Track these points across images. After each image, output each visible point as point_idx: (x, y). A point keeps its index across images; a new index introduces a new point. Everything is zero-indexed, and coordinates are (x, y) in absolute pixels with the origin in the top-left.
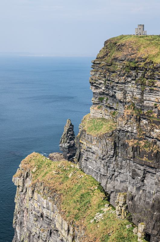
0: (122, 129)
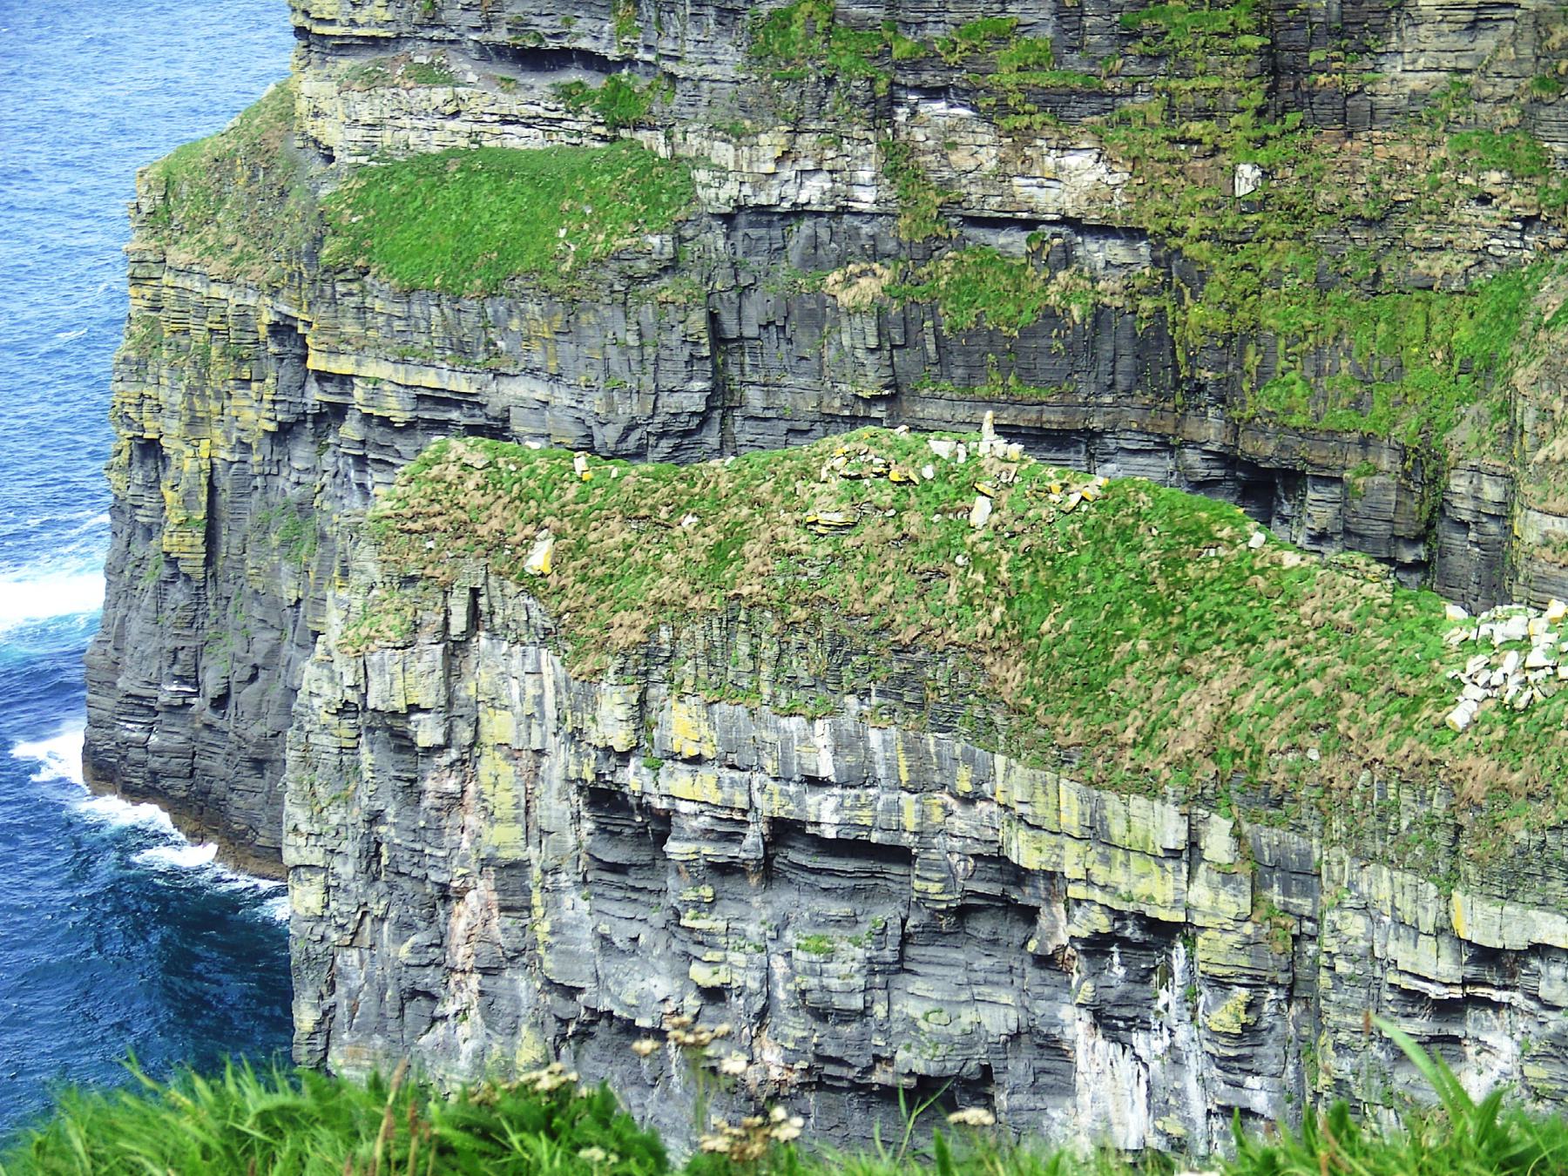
0: (752, 202)
